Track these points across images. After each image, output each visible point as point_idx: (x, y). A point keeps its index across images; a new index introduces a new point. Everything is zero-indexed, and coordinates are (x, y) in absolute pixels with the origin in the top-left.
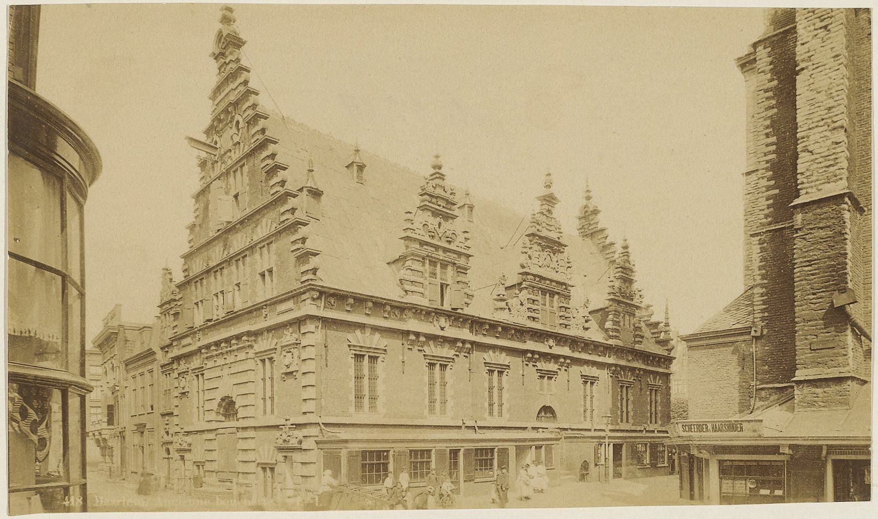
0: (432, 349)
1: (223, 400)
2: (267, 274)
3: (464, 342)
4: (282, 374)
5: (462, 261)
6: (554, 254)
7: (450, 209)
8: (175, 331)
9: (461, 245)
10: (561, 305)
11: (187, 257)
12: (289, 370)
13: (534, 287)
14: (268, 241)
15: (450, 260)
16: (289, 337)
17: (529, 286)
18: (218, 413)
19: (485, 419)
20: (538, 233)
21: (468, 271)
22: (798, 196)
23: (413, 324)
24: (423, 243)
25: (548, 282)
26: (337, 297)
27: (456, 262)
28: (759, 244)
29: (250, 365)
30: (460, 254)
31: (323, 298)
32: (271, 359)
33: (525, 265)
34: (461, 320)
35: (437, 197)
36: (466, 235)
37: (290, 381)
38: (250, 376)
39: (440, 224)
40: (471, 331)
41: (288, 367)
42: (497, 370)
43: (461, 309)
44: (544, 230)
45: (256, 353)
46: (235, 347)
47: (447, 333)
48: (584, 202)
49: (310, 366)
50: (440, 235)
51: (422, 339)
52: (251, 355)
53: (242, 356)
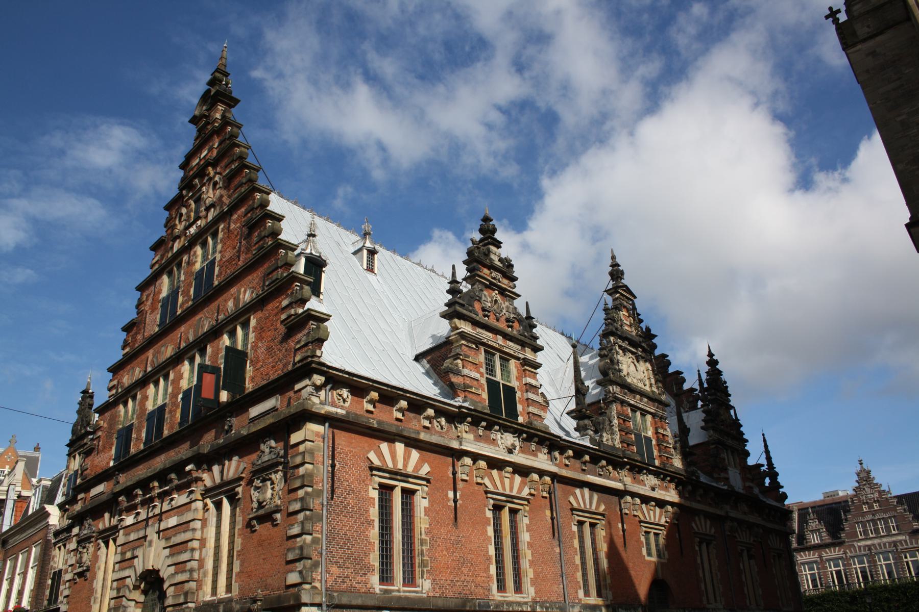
11: (116, 369)
12: (261, 512)
14: (241, 316)
32: (233, 500)
47: (519, 458)
51: (482, 464)
53: (180, 499)
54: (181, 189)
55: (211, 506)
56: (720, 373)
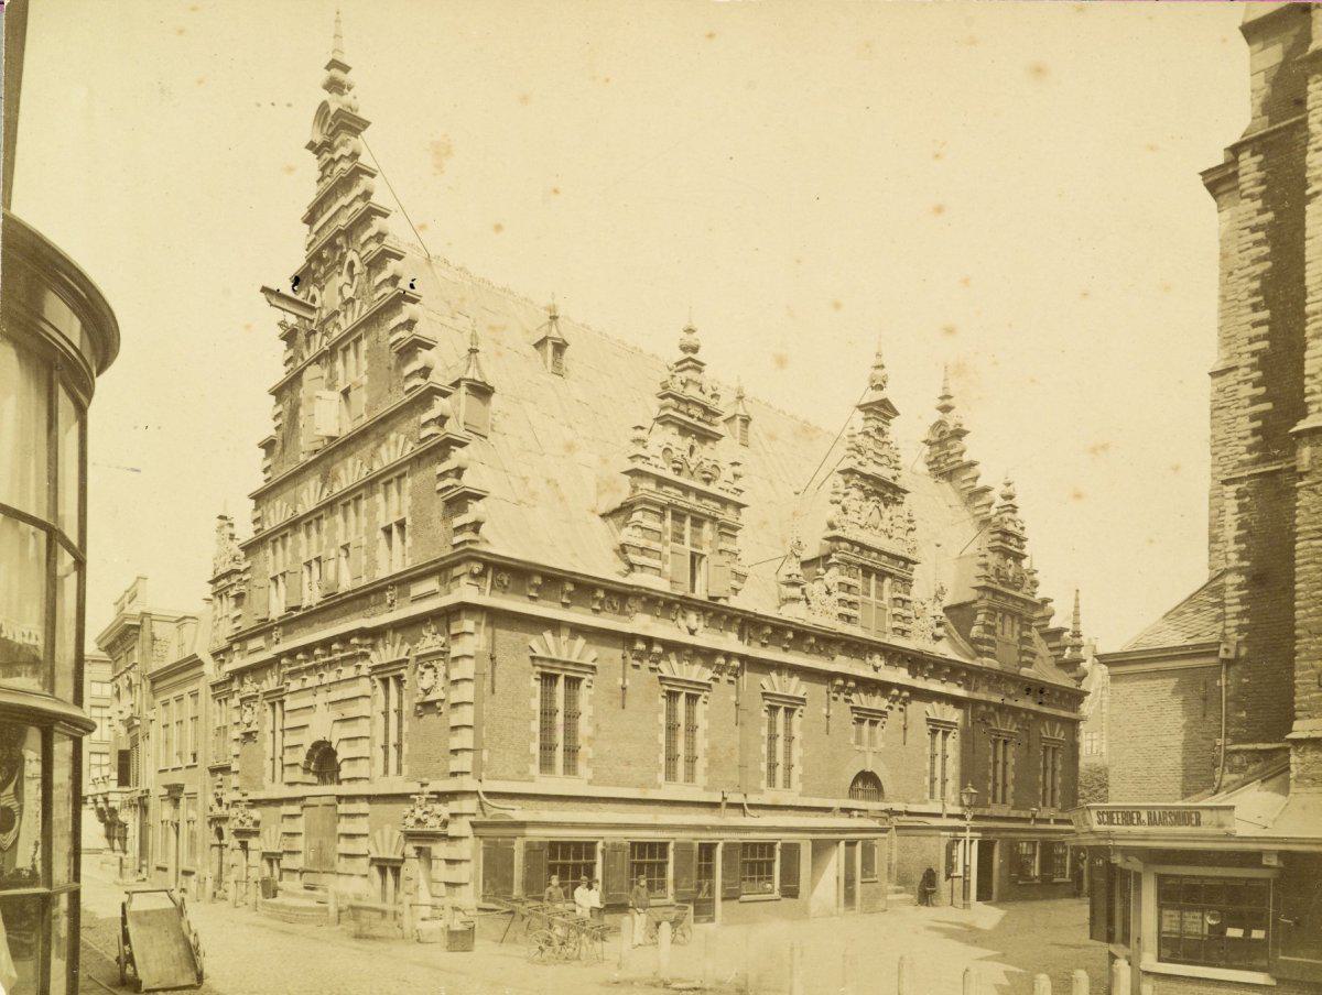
0: (673, 668)
1: (317, 745)
2: (395, 529)
3: (728, 656)
4: (418, 704)
5: (729, 515)
6: (886, 506)
7: (710, 424)
8: (236, 625)
9: (727, 486)
10: (896, 595)
13: (849, 563)
15: (707, 512)
16: (430, 641)
17: (844, 560)
18: (306, 770)
19: (761, 792)
20: (861, 469)
21: (738, 533)
22: (1304, 415)
23: (641, 623)
24: (661, 482)
25: (874, 554)
26: (514, 573)
27: (718, 516)
28: (1236, 498)
29: (364, 686)
30: (724, 502)
31: (490, 574)
33: (836, 523)
34: (725, 617)
35: (687, 402)
36: (737, 469)
37: (430, 718)
38: (362, 708)
39: (692, 449)
40: (741, 638)
41: (427, 692)
42: (784, 706)
43: (726, 598)
44: (870, 463)
45: (374, 668)
46: (338, 656)
48: (938, 416)
49: (466, 692)
50: (692, 468)
51: (657, 649)
52: (365, 671)
54: (310, 261)
55: (378, 683)
56: (1014, 509)
